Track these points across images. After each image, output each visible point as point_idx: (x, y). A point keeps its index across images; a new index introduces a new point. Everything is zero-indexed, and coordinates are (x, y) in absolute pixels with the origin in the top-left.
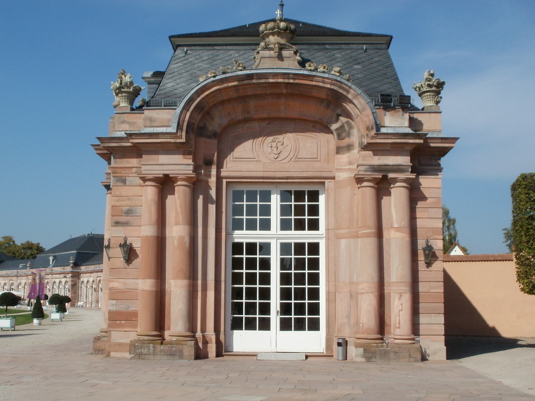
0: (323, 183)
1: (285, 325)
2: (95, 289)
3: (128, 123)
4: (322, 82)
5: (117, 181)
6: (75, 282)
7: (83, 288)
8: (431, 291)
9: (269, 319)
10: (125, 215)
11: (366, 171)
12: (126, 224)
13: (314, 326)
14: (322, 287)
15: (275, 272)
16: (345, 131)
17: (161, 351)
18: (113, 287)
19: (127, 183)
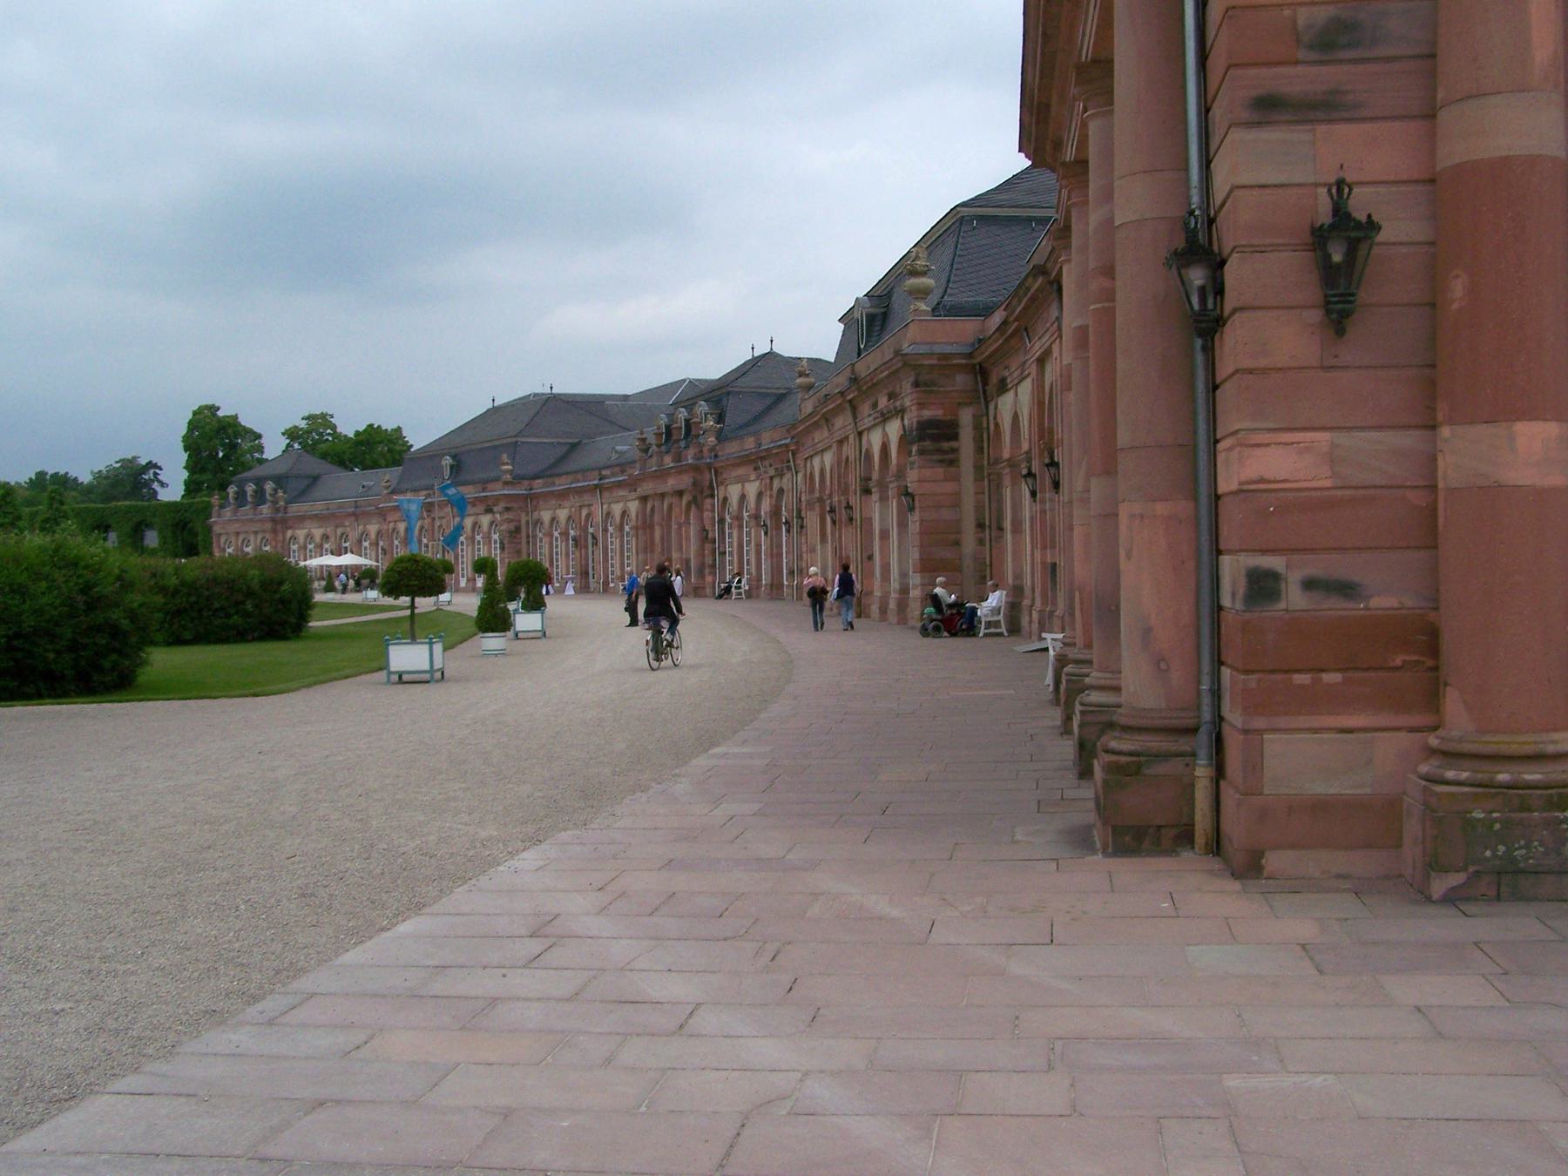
2: (574, 539)
6: (517, 524)
7: (557, 538)
10: (1313, 56)
18: (1262, 480)
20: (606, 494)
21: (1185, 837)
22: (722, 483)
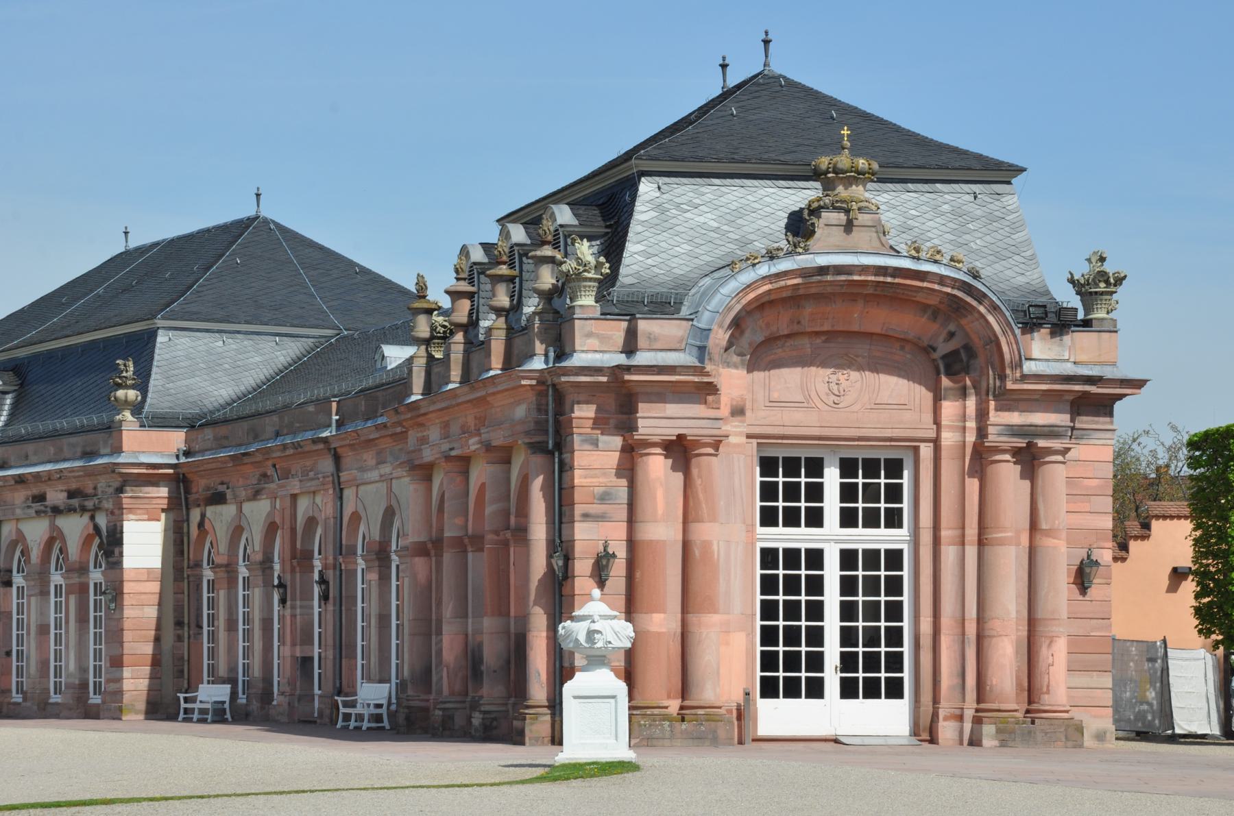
1: (848, 690)
3: (597, 336)
4: (939, 284)
5: (584, 441)
8: (1092, 634)
9: (821, 680)
10: (599, 502)
11: (999, 435)
13: (895, 690)
15: (832, 598)
16: (961, 361)
17: (682, 732)
19: (600, 445)
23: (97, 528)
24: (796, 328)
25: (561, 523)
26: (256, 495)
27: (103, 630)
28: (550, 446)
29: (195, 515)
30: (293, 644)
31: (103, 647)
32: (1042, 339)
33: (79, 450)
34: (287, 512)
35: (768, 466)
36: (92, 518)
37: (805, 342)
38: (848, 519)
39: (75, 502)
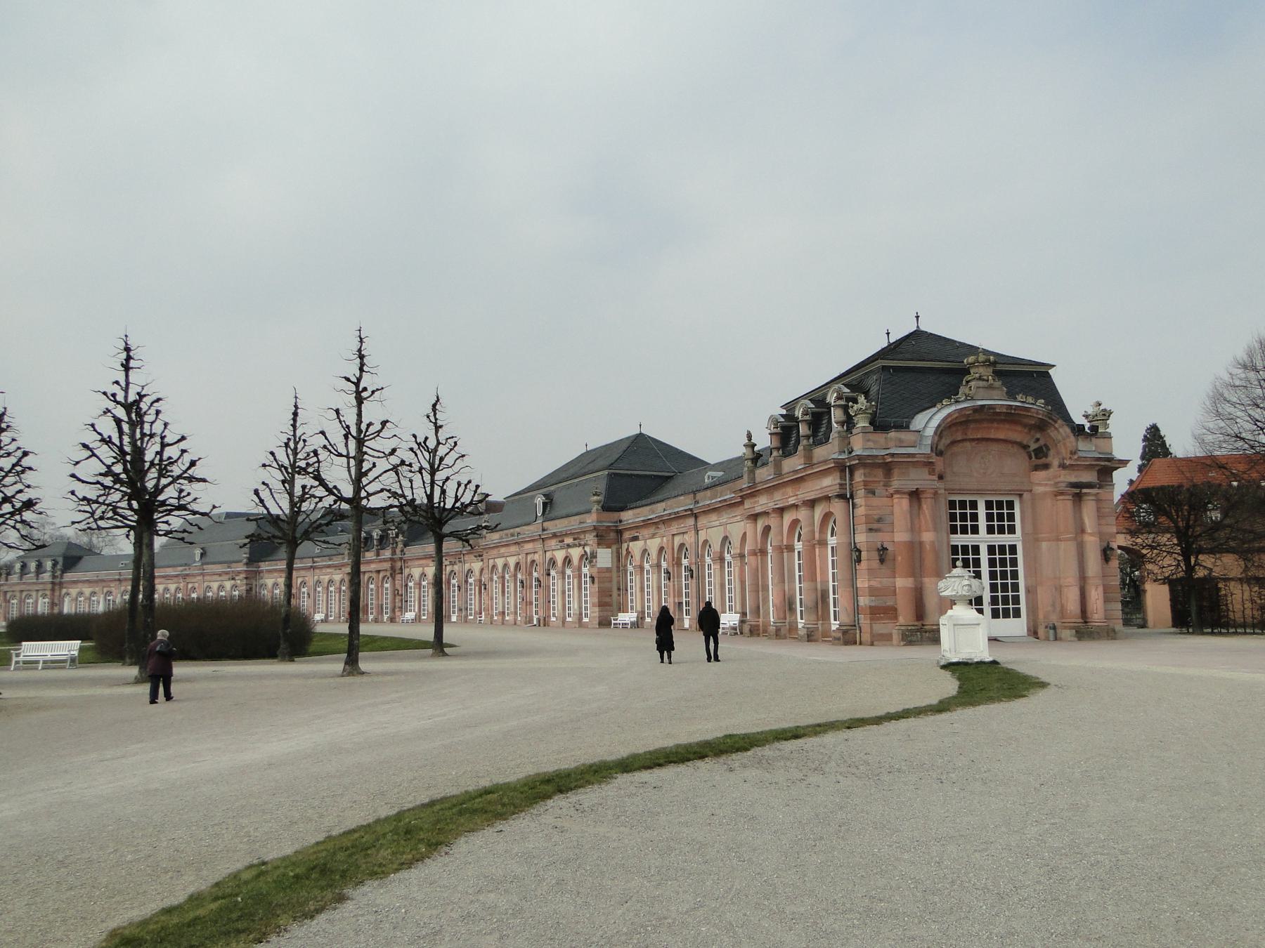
0: (1021, 496)
1: (995, 614)
5: (868, 492)
11: (1067, 487)
12: (877, 530)
13: (1017, 614)
14: (1021, 581)
16: (1043, 452)
20: (317, 571)
21: (855, 643)
22: (408, 567)
23: (585, 552)
24: (965, 437)
25: (854, 534)
26: (653, 536)
27: (588, 592)
28: (848, 496)
29: (625, 546)
30: (674, 597)
31: (588, 599)
32: (1083, 441)
33: (578, 521)
34: (671, 541)
35: (952, 504)
36: (584, 548)
37: (968, 444)
38: (990, 530)
39: (576, 542)
